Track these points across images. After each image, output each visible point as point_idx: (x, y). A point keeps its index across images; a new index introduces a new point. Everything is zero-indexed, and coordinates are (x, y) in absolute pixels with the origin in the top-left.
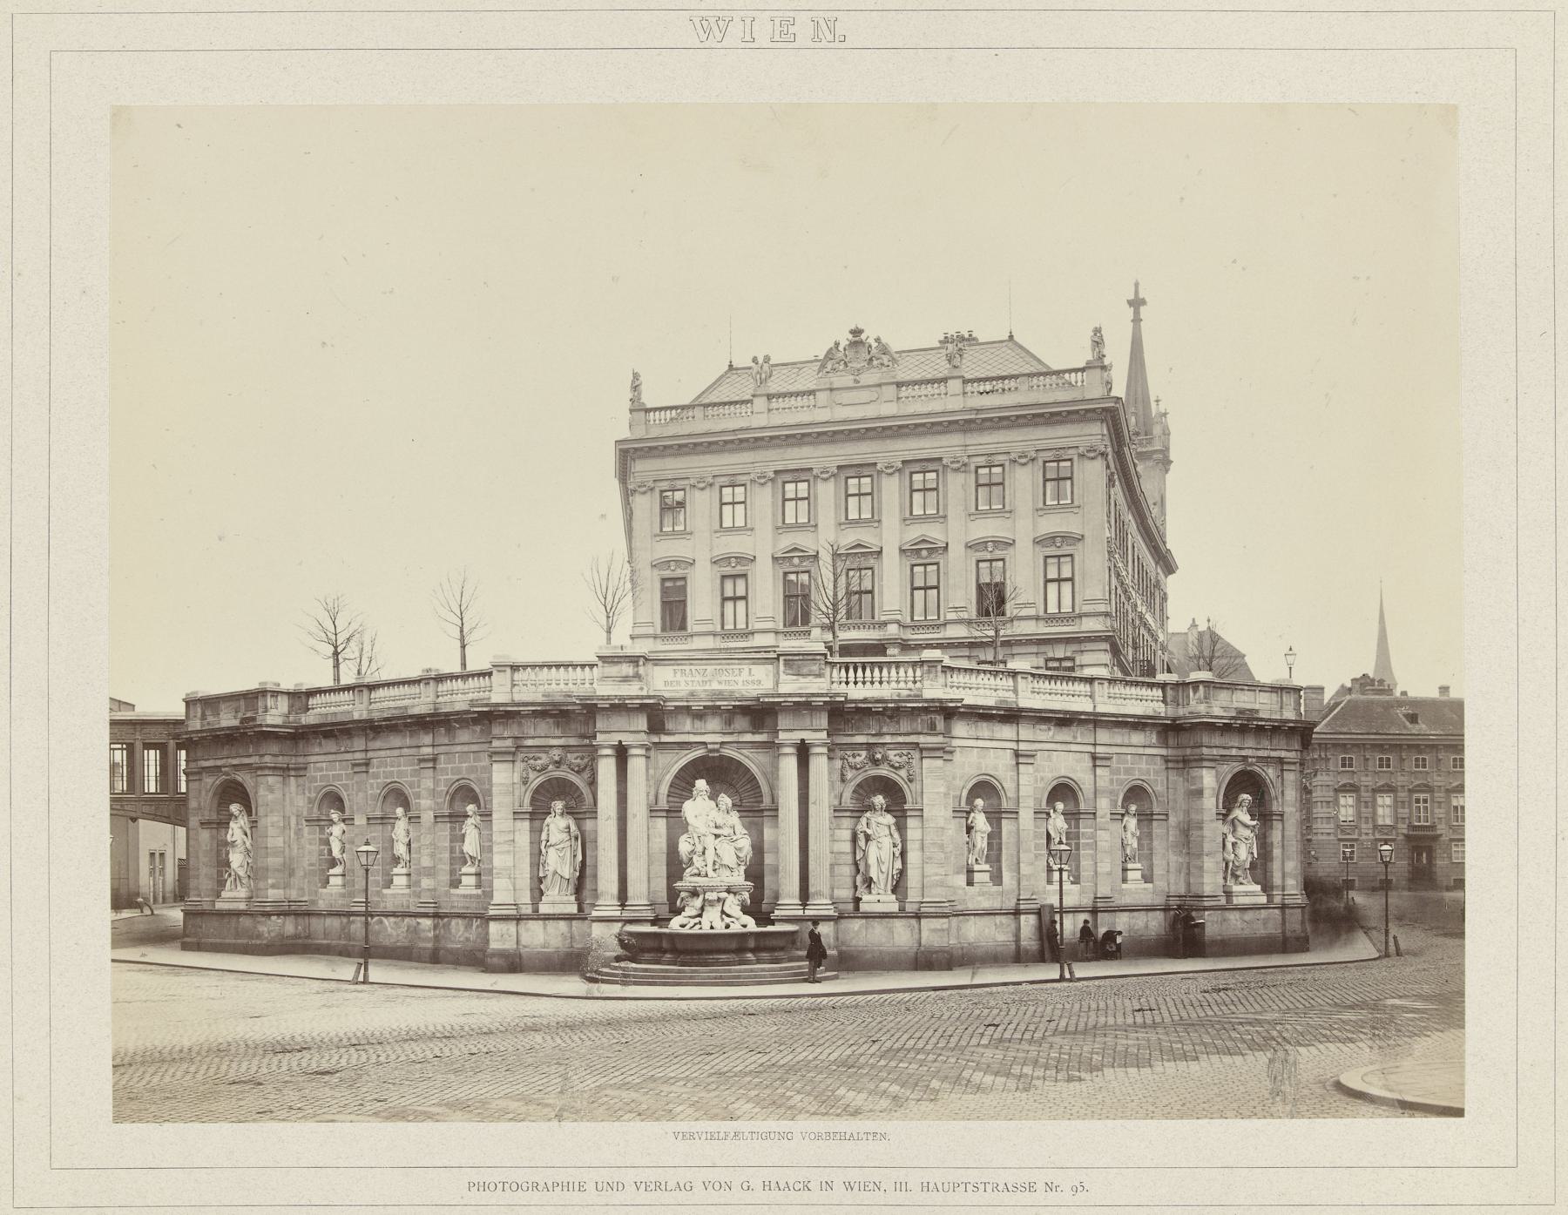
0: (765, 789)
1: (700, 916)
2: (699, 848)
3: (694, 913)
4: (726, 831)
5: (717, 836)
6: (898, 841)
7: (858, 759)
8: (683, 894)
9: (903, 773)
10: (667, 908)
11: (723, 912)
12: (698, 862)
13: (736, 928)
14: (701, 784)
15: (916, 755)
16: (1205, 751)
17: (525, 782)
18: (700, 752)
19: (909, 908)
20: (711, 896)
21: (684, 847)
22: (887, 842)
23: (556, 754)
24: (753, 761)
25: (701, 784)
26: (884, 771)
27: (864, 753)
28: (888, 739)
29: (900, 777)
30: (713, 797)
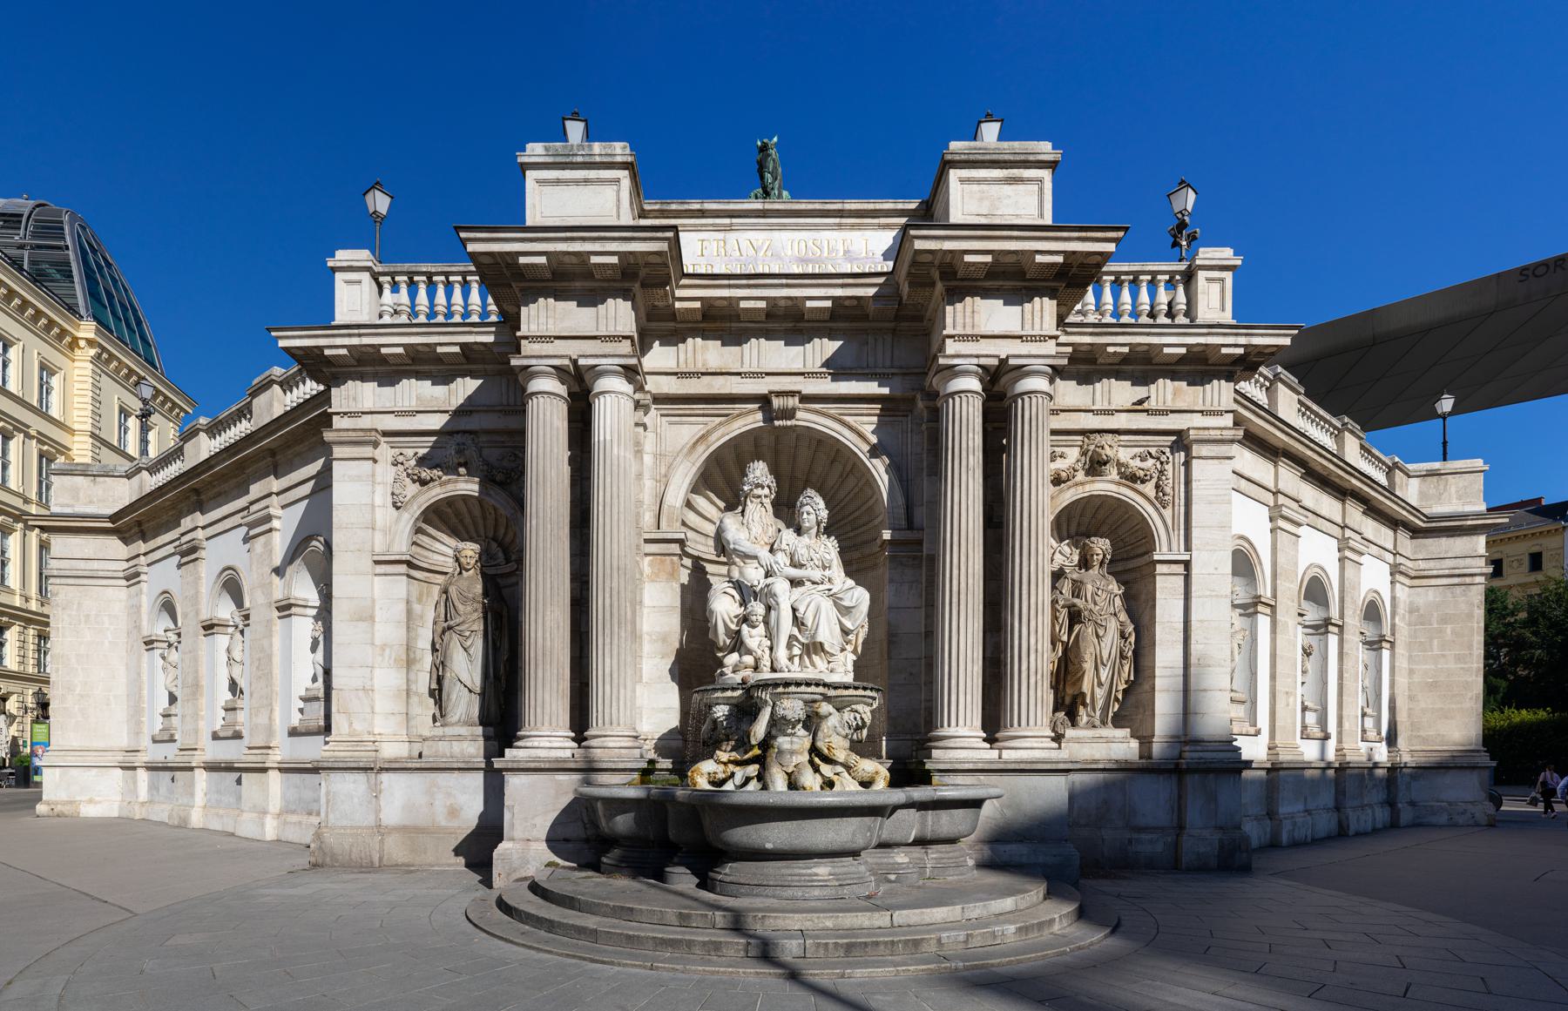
4: (817, 574)
6: (1130, 628)
7: (1060, 464)
11: (814, 750)
12: (754, 638)
13: (847, 790)
14: (759, 471)
18: (753, 420)
20: (792, 707)
25: (759, 471)
26: (1107, 485)
27: (1073, 454)
29: (1139, 500)
30: (786, 509)
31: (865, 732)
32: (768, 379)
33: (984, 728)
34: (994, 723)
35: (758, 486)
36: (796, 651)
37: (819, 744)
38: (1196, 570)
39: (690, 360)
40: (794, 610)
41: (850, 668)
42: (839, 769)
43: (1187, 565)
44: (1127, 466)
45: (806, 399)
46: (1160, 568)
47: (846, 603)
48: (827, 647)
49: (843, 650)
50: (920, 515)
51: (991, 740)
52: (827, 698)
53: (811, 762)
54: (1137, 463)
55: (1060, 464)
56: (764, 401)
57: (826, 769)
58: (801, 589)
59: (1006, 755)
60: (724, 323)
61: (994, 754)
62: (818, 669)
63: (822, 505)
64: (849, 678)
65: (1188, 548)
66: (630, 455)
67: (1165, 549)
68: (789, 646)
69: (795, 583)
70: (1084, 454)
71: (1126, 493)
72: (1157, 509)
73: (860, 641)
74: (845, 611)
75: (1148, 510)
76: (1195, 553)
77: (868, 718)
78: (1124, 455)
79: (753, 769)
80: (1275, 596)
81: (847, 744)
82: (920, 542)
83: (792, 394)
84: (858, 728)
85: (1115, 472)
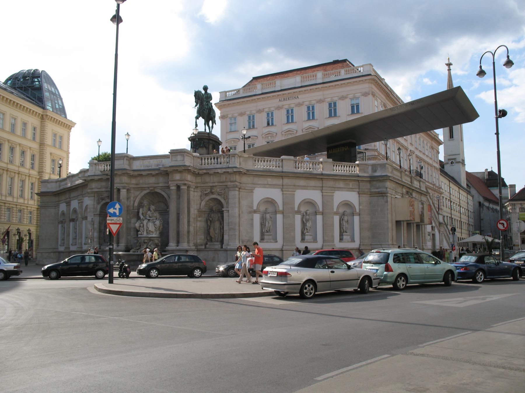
2: (142, 225)
5: (149, 220)
18: (148, 191)
28: (216, 184)
34: (178, 242)
55: (207, 192)
68: (147, 230)
71: (219, 197)
75: (222, 201)
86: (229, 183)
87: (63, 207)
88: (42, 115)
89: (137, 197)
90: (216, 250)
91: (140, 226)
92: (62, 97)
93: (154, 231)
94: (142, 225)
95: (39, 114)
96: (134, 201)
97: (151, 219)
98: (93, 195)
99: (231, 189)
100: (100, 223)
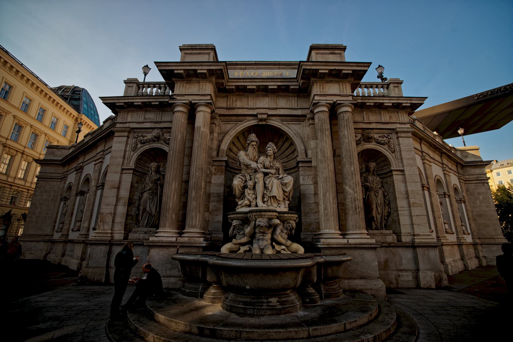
0: (300, 147)
1: (250, 243)
2: (250, 183)
3: (244, 240)
8: (235, 223)
9: (386, 147)
10: (221, 236)
11: (273, 240)
14: (253, 137)
15: (394, 136)
16: (467, 177)
17: (135, 149)
18: (253, 122)
19: (405, 239)
21: (237, 182)
22: (380, 192)
23: (155, 133)
24: (291, 129)
28: (374, 126)
30: (262, 151)
31: (294, 231)
32: (257, 110)
33: (340, 230)
35: (252, 141)
36: (265, 199)
37: (275, 237)
38: (406, 173)
39: (231, 105)
40: (265, 184)
41: (287, 206)
42: (283, 247)
43: (402, 171)
44: (377, 140)
45: (269, 116)
46: (394, 173)
47: (285, 181)
48: (277, 198)
49: (284, 199)
50: (309, 152)
51: (344, 235)
52: (278, 218)
53: (272, 244)
54: (381, 139)
56: (256, 116)
57: (277, 247)
58: (268, 176)
59: (351, 241)
60: (242, 91)
61: (345, 241)
62: (274, 206)
63: (275, 147)
64: (286, 210)
65: (403, 166)
66: (208, 131)
67: (395, 166)
68: (263, 197)
69: (266, 174)
70: (363, 135)
72: (390, 153)
73: (291, 196)
74: (284, 185)
75: (387, 153)
76: (405, 167)
77: (294, 225)
78: (376, 136)
79: (246, 248)
80: (428, 184)
81: (286, 236)
82: (311, 162)
83: (264, 114)
84: (291, 230)
85: (374, 141)
86: (398, 126)
87: (72, 178)
88: (77, 118)
89: (226, 133)
90: (390, 246)
91: (245, 187)
92: (99, 114)
93: (281, 199)
94: (250, 183)
95: (74, 116)
96: (220, 142)
97: (273, 171)
98: (126, 134)
99: (402, 135)
100: (132, 186)
